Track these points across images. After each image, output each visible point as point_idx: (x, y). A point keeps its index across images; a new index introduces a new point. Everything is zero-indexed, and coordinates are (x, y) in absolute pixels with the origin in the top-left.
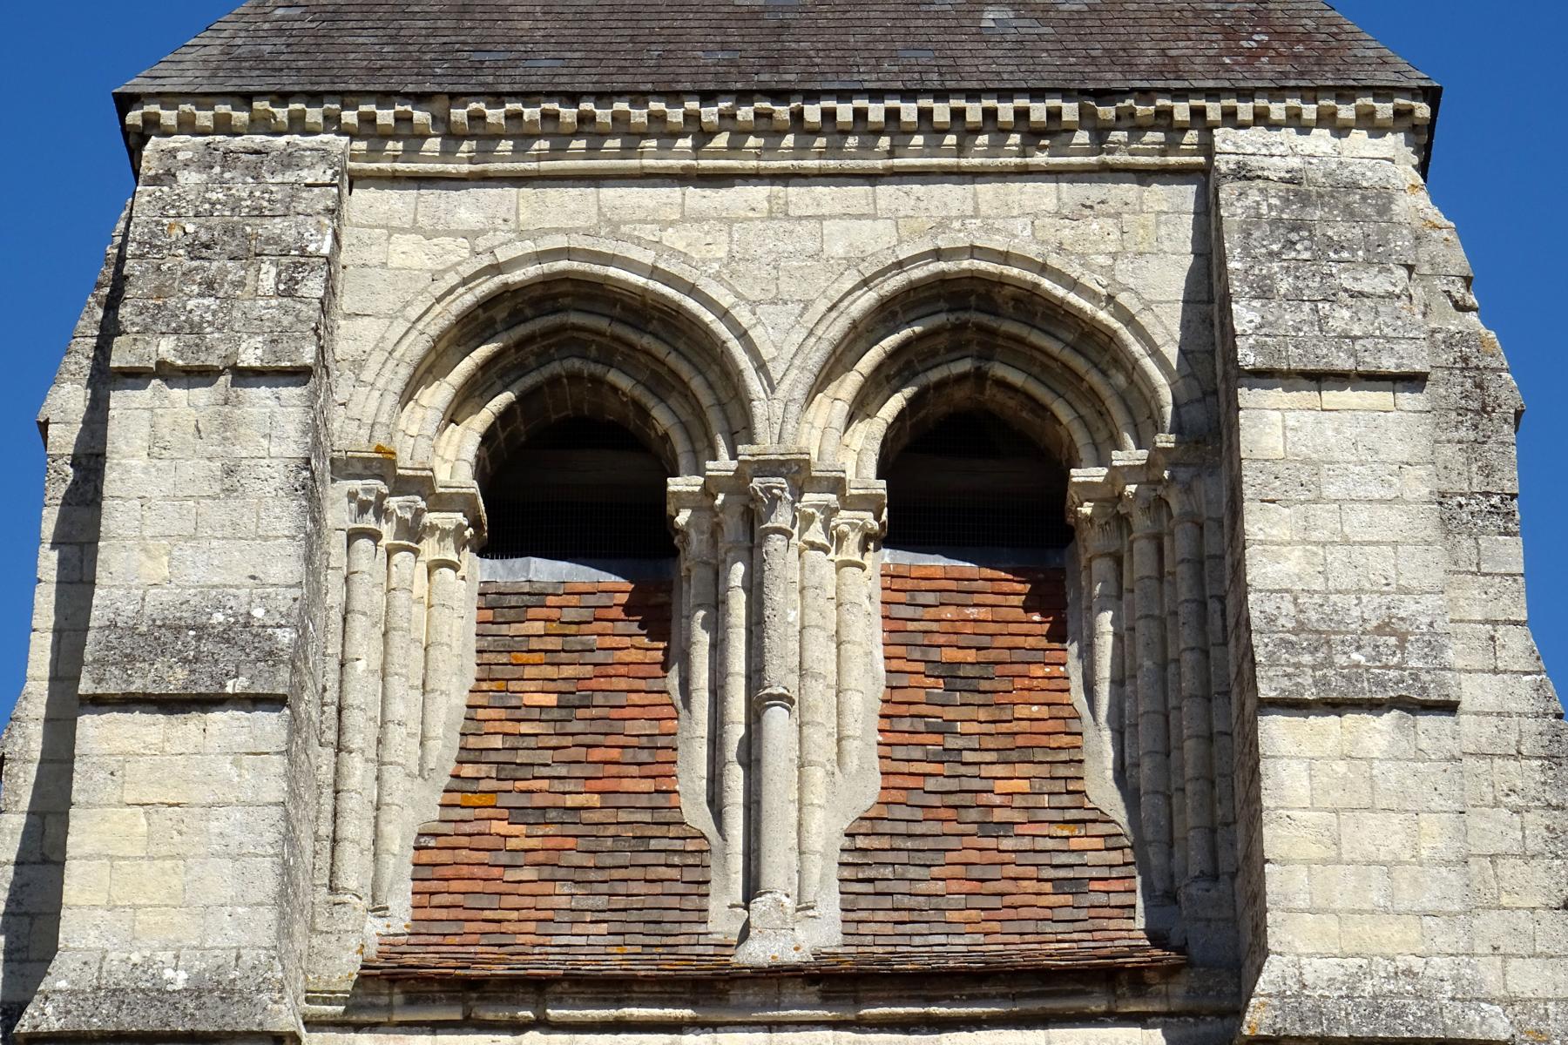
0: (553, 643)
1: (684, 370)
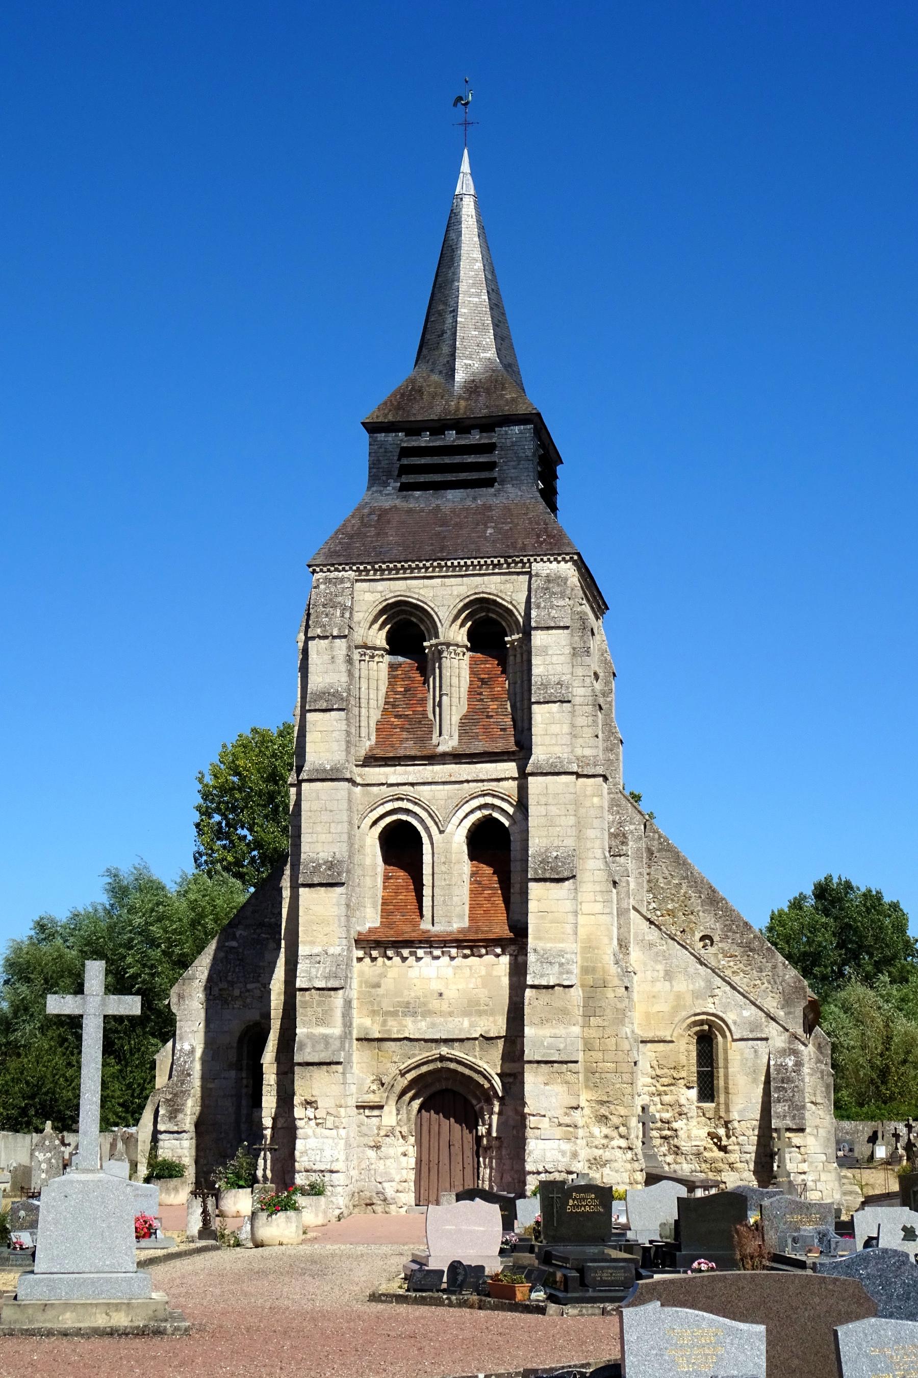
0: (403, 676)
1: (426, 619)
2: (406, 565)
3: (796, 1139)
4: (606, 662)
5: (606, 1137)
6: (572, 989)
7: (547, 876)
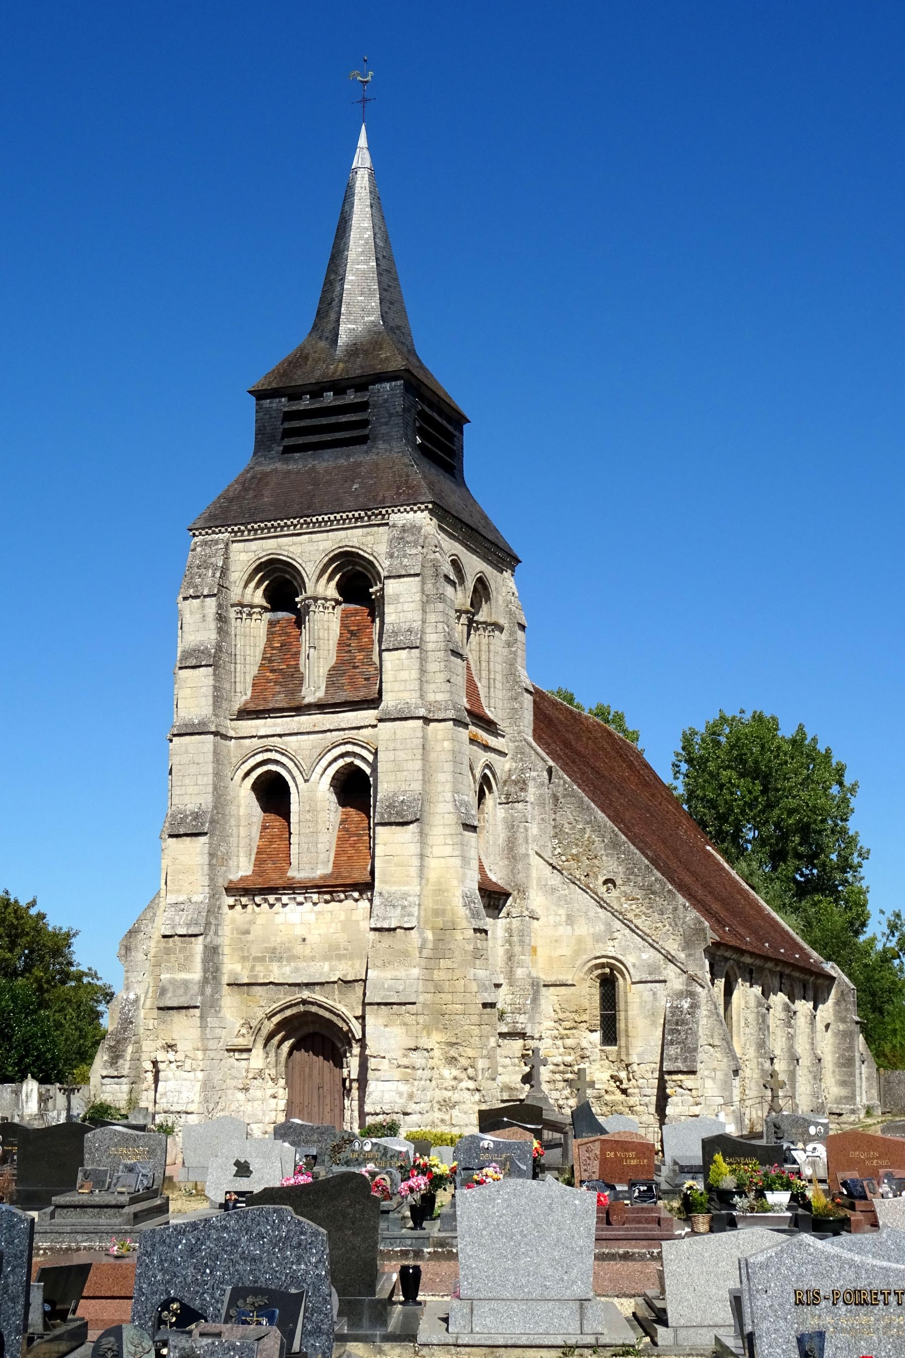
2: (276, 524)
3: (688, 1081)
4: (510, 613)
5: (455, 1078)
6: (412, 931)
7: (393, 820)
